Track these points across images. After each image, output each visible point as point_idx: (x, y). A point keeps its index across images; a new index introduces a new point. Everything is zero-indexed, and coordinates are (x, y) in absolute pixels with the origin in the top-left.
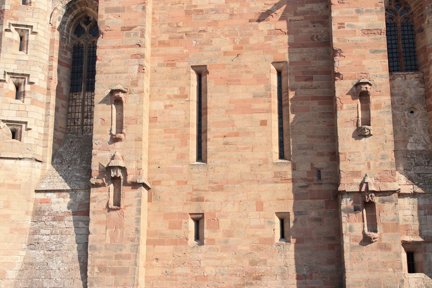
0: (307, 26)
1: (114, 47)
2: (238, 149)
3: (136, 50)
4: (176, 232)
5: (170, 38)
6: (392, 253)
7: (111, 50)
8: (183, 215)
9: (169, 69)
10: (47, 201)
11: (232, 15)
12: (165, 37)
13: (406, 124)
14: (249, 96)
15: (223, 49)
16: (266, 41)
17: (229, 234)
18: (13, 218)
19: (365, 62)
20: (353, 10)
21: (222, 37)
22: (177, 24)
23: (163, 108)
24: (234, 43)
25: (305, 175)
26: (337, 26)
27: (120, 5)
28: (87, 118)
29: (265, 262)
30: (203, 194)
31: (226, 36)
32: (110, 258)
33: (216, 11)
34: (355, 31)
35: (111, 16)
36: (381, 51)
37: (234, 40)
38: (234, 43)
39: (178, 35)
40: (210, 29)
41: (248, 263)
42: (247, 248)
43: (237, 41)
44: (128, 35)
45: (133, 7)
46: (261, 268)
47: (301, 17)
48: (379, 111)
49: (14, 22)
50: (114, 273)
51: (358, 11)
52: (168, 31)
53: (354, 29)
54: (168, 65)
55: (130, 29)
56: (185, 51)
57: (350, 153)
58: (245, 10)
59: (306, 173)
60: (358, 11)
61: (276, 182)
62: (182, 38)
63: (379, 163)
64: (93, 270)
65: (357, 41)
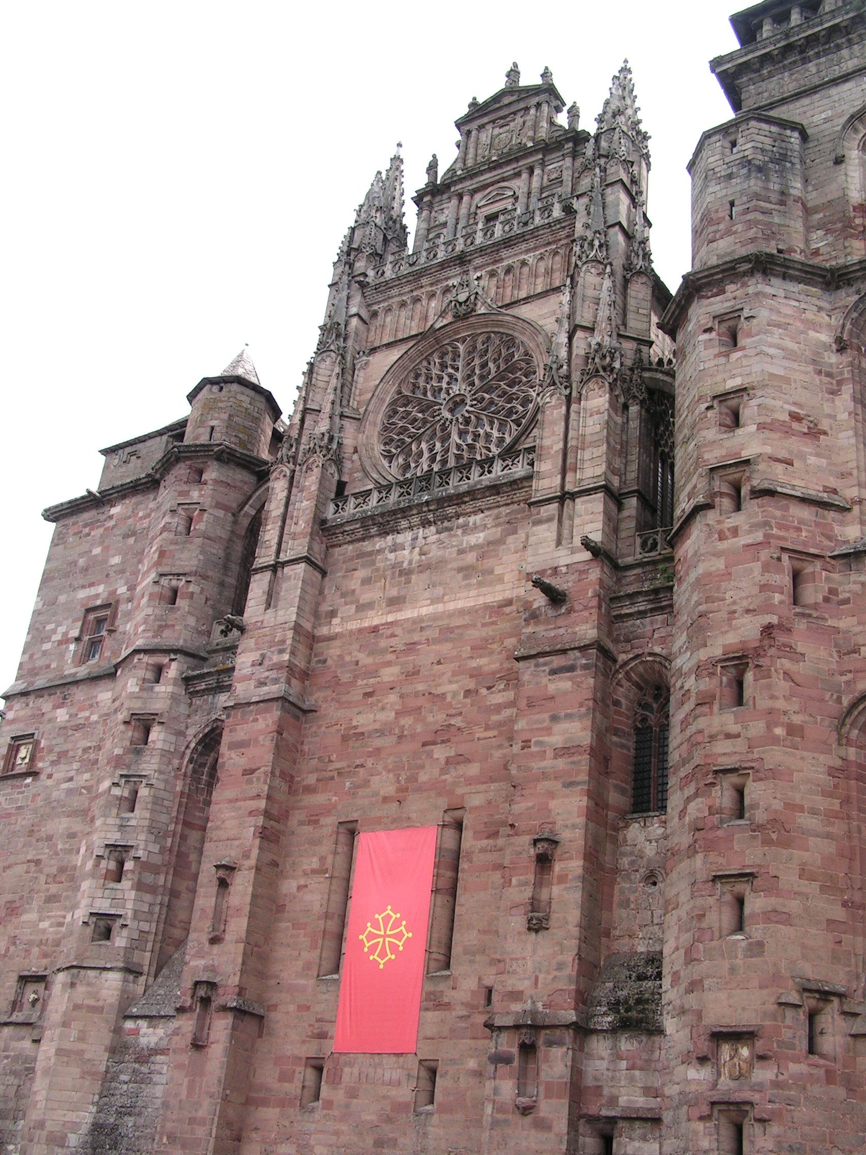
0: (500, 746)
1: (230, 801)
5: (318, 780)
6: (552, 1136)
7: (226, 805)
9: (310, 828)
11: (401, 737)
12: (311, 779)
15: (382, 793)
16: (441, 774)
18: (87, 1056)
19: (553, 804)
21: (384, 773)
22: (329, 757)
23: (295, 889)
24: (398, 782)
26: (520, 744)
27: (246, 737)
31: (389, 771)
33: (381, 732)
34: (545, 752)
35: (233, 755)
36: (578, 783)
37: (398, 776)
38: (398, 782)
40: (369, 763)
41: (372, 1142)
43: (402, 778)
44: (250, 782)
45: (261, 738)
47: (495, 733)
48: (563, 886)
51: (554, 718)
52: (317, 770)
53: (543, 749)
54: (310, 823)
55: (252, 771)
56: (334, 799)
57: (512, 959)
58: (419, 728)
59: (469, 994)
61: (427, 1009)
62: (332, 778)
63: (551, 977)
64: (161, 1139)
65: (545, 768)
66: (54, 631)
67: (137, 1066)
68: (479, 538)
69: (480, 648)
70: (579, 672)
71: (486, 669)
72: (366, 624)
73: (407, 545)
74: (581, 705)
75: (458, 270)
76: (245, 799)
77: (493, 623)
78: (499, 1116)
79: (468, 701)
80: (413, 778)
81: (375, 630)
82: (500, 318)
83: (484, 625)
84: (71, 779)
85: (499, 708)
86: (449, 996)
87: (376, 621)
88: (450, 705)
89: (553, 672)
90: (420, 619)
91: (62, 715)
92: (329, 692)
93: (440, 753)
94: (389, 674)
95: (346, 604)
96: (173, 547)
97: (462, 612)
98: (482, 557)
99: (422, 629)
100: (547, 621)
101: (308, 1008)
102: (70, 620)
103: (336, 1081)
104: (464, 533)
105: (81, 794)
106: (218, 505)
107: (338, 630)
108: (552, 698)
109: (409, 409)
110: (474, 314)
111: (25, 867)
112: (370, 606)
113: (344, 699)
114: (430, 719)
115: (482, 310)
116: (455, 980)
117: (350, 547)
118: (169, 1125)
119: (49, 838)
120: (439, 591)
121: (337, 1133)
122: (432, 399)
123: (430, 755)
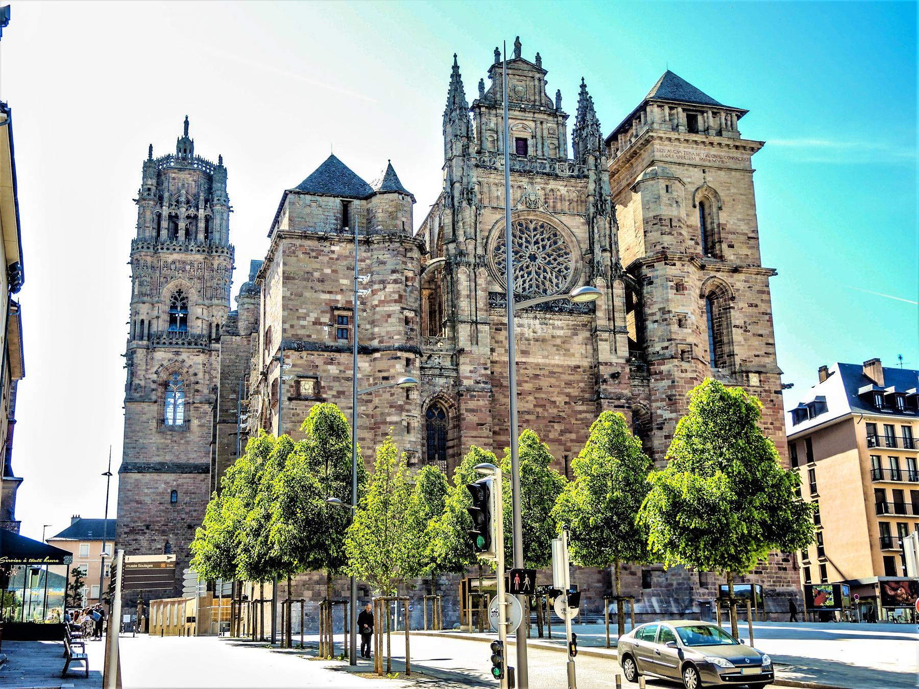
0: (583, 429)
1: (473, 437)
3: (487, 440)
12: (497, 428)
27: (475, 408)
33: (528, 413)
39: (504, 427)
44: (482, 429)
45: (483, 409)
52: (498, 425)
54: (499, 448)
55: (482, 425)
58: (546, 415)
66: (307, 315)
68: (561, 333)
69: (569, 384)
71: (573, 394)
73: (526, 325)
76: (481, 437)
77: (573, 374)
79: (567, 406)
82: (552, 218)
83: (569, 374)
85: (581, 412)
88: (558, 407)
89: (615, 407)
90: (538, 365)
91: (333, 370)
92: (497, 389)
93: (556, 426)
96: (404, 294)
97: (558, 366)
99: (540, 369)
100: (611, 385)
102: (319, 312)
104: (553, 328)
105: (362, 417)
107: (497, 359)
114: (550, 411)
115: (541, 209)
117: (496, 318)
120: (546, 353)
123: (553, 427)
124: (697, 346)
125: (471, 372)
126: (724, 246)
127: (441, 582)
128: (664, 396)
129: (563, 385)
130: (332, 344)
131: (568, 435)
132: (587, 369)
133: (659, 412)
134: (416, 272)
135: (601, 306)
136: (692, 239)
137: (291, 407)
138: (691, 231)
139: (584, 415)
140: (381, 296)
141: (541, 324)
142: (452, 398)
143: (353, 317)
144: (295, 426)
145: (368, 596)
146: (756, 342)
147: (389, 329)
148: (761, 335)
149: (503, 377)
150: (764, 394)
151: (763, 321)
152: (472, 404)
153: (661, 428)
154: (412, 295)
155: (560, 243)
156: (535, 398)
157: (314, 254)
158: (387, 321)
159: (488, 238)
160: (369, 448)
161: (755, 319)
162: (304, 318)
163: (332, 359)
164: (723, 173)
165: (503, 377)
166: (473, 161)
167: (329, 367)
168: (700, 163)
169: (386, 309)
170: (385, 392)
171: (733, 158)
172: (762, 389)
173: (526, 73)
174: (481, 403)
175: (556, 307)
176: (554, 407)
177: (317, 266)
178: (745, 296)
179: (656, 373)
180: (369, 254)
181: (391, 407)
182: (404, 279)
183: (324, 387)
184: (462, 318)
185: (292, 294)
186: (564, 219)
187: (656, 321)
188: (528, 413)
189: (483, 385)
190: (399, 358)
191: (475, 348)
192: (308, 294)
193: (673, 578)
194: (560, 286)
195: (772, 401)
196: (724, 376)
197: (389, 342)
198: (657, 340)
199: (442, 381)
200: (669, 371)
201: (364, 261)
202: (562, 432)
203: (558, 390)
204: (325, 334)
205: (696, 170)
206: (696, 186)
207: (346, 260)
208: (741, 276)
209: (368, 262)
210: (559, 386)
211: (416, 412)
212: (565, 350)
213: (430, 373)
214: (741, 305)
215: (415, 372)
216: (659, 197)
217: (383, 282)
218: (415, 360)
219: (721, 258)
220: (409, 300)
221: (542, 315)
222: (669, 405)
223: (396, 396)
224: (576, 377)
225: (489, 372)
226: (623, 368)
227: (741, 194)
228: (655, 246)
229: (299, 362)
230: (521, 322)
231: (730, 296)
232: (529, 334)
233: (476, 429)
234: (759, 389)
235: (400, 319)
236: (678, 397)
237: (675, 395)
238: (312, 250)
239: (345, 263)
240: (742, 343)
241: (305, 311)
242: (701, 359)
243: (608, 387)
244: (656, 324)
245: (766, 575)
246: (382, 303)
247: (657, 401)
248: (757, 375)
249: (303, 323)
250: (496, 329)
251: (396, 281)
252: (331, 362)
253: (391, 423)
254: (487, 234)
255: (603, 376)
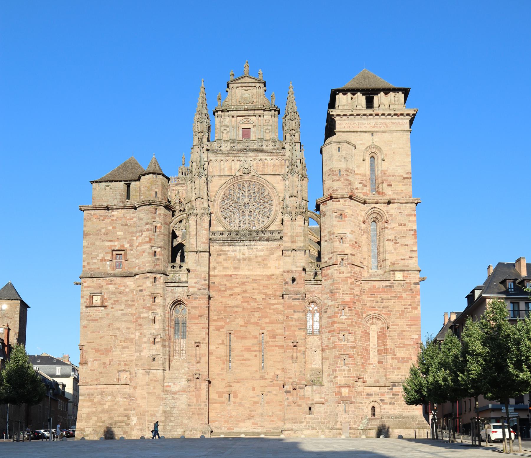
0: (274, 315)
2: (246, 366)
4: (221, 399)
8: (223, 392)
9: (217, 332)
10: (169, 386)
11: (243, 309)
12: (216, 318)
13: (312, 357)
14: (250, 344)
17: (241, 400)
20: (292, 311)
23: (215, 348)
25: (272, 377)
28: (182, 350)
29: (255, 411)
30: (231, 384)
31: (241, 318)
32: (196, 409)
33: (237, 307)
36: (303, 329)
39: (221, 317)
40: (234, 315)
42: (248, 405)
43: (246, 320)
44: (201, 319)
45: (203, 306)
46: (253, 413)
47: (273, 311)
49: (153, 312)
50: (198, 414)
51: (294, 312)
52: (217, 315)
55: (201, 316)
56: (224, 324)
58: (249, 307)
60: (294, 312)
64: (190, 414)
66: (97, 256)
67: (173, 395)
68: (262, 254)
69: (265, 286)
70: (301, 300)
71: (268, 293)
72: (227, 274)
73: (238, 251)
74: (302, 309)
75: (243, 155)
76: (200, 324)
77: (269, 280)
78: (289, 404)
79: (264, 301)
80: (249, 321)
81: (231, 276)
83: (266, 280)
84: (122, 310)
85: (273, 304)
86: (266, 377)
87: (230, 273)
88: (258, 302)
89: (294, 299)
90: (245, 275)
91: (112, 288)
92: (217, 293)
93: (256, 314)
94: (237, 290)
95: (219, 266)
96: (153, 237)
97: (259, 275)
98: (263, 260)
100: (290, 285)
101: (225, 379)
103: (236, 396)
106: (166, 223)
108: (293, 306)
109: (229, 201)
110: (250, 174)
111: (110, 337)
112: (227, 268)
113: (223, 295)
115: (253, 173)
116: (268, 373)
117: (218, 247)
118: (192, 410)
119: (118, 329)
120: (251, 267)
121: (238, 409)
122: (236, 200)
123: (253, 315)
124: (354, 255)
125: (195, 283)
126: (385, 185)
127: (174, 412)
128: (328, 291)
129: (262, 287)
130: (112, 272)
131: (264, 320)
132: (279, 276)
133: (326, 301)
134: (163, 223)
135: (287, 234)
136: (360, 183)
137: (87, 311)
138: (360, 177)
139: (275, 306)
140: (140, 240)
141: (248, 249)
142: (186, 300)
143: (126, 255)
144: (89, 322)
145: (129, 420)
146: (403, 250)
147: (143, 260)
148: (407, 245)
149: (221, 285)
150: (405, 285)
151: (410, 235)
152: (195, 303)
153: (326, 312)
154: (159, 237)
155: (266, 194)
156: (242, 297)
157: (102, 218)
158: (142, 255)
159: (215, 196)
160: (132, 334)
161: (403, 234)
162: (96, 258)
163: (111, 281)
164: (386, 135)
165: (221, 285)
166: (205, 147)
167: (110, 286)
168: (370, 130)
169: (143, 247)
170: (140, 299)
171: (395, 123)
172: (404, 282)
173: (250, 85)
174: (202, 302)
175: (257, 237)
176: (255, 302)
177: (104, 225)
178: (396, 219)
179: (325, 276)
180: (135, 215)
181: (144, 308)
182: (153, 228)
183: (106, 299)
184: (191, 249)
185: (88, 244)
186: (267, 178)
187: (326, 241)
188: (237, 307)
189: (203, 291)
190: (148, 277)
191: (198, 268)
192: (97, 243)
193: (328, 408)
194: (265, 223)
195: (411, 290)
196: (378, 275)
197: (143, 268)
198: (326, 253)
199: (180, 290)
200: (332, 274)
201: (131, 219)
202: (260, 318)
203: (258, 291)
204: (108, 267)
205: (366, 134)
206: (366, 146)
207: (121, 220)
208: (395, 205)
209: (135, 219)
210: (259, 289)
211: (160, 310)
212: (264, 265)
213: (172, 285)
214: (393, 225)
215: (160, 286)
216: (332, 156)
217: (141, 231)
218: (160, 278)
219: (383, 194)
220: (156, 240)
221: (248, 243)
222: (331, 296)
223: (146, 301)
224: (272, 282)
225: (207, 282)
226: (300, 273)
227: (400, 148)
228: (329, 190)
229: (92, 284)
230: (235, 249)
231: (385, 220)
232: (239, 256)
233: (198, 319)
234: (402, 282)
235: (149, 253)
236: (336, 291)
237: (334, 290)
238: (101, 216)
239: (120, 222)
240: (392, 251)
241: (96, 253)
242: (360, 265)
243: (289, 287)
244: (326, 242)
245: (397, 405)
246: (140, 244)
247: (325, 294)
248: (402, 272)
249: (95, 261)
250: (218, 255)
251: (148, 230)
252: (111, 283)
253: (143, 318)
254: (214, 194)
255: (285, 280)
